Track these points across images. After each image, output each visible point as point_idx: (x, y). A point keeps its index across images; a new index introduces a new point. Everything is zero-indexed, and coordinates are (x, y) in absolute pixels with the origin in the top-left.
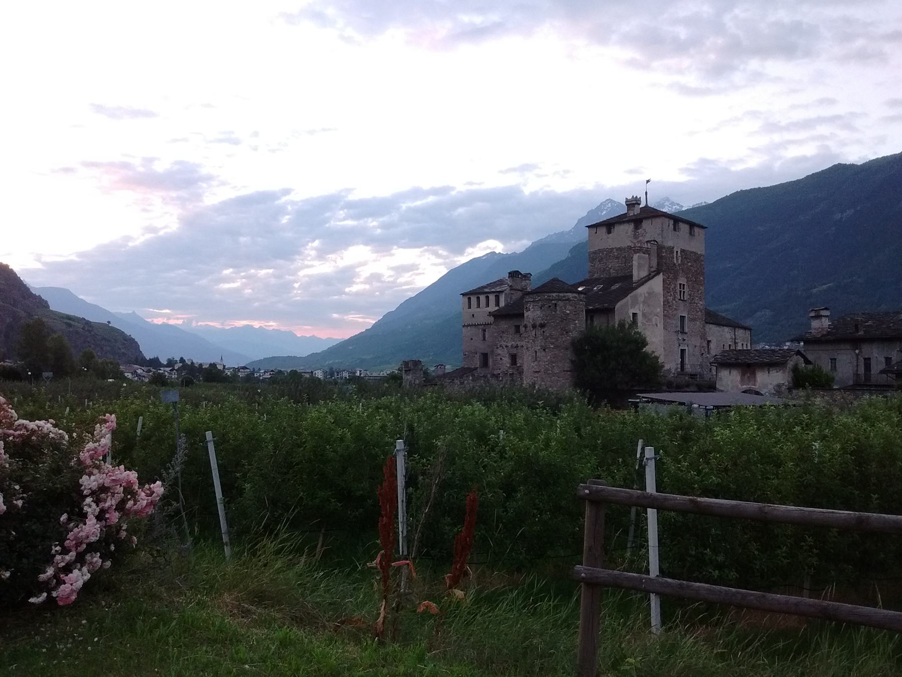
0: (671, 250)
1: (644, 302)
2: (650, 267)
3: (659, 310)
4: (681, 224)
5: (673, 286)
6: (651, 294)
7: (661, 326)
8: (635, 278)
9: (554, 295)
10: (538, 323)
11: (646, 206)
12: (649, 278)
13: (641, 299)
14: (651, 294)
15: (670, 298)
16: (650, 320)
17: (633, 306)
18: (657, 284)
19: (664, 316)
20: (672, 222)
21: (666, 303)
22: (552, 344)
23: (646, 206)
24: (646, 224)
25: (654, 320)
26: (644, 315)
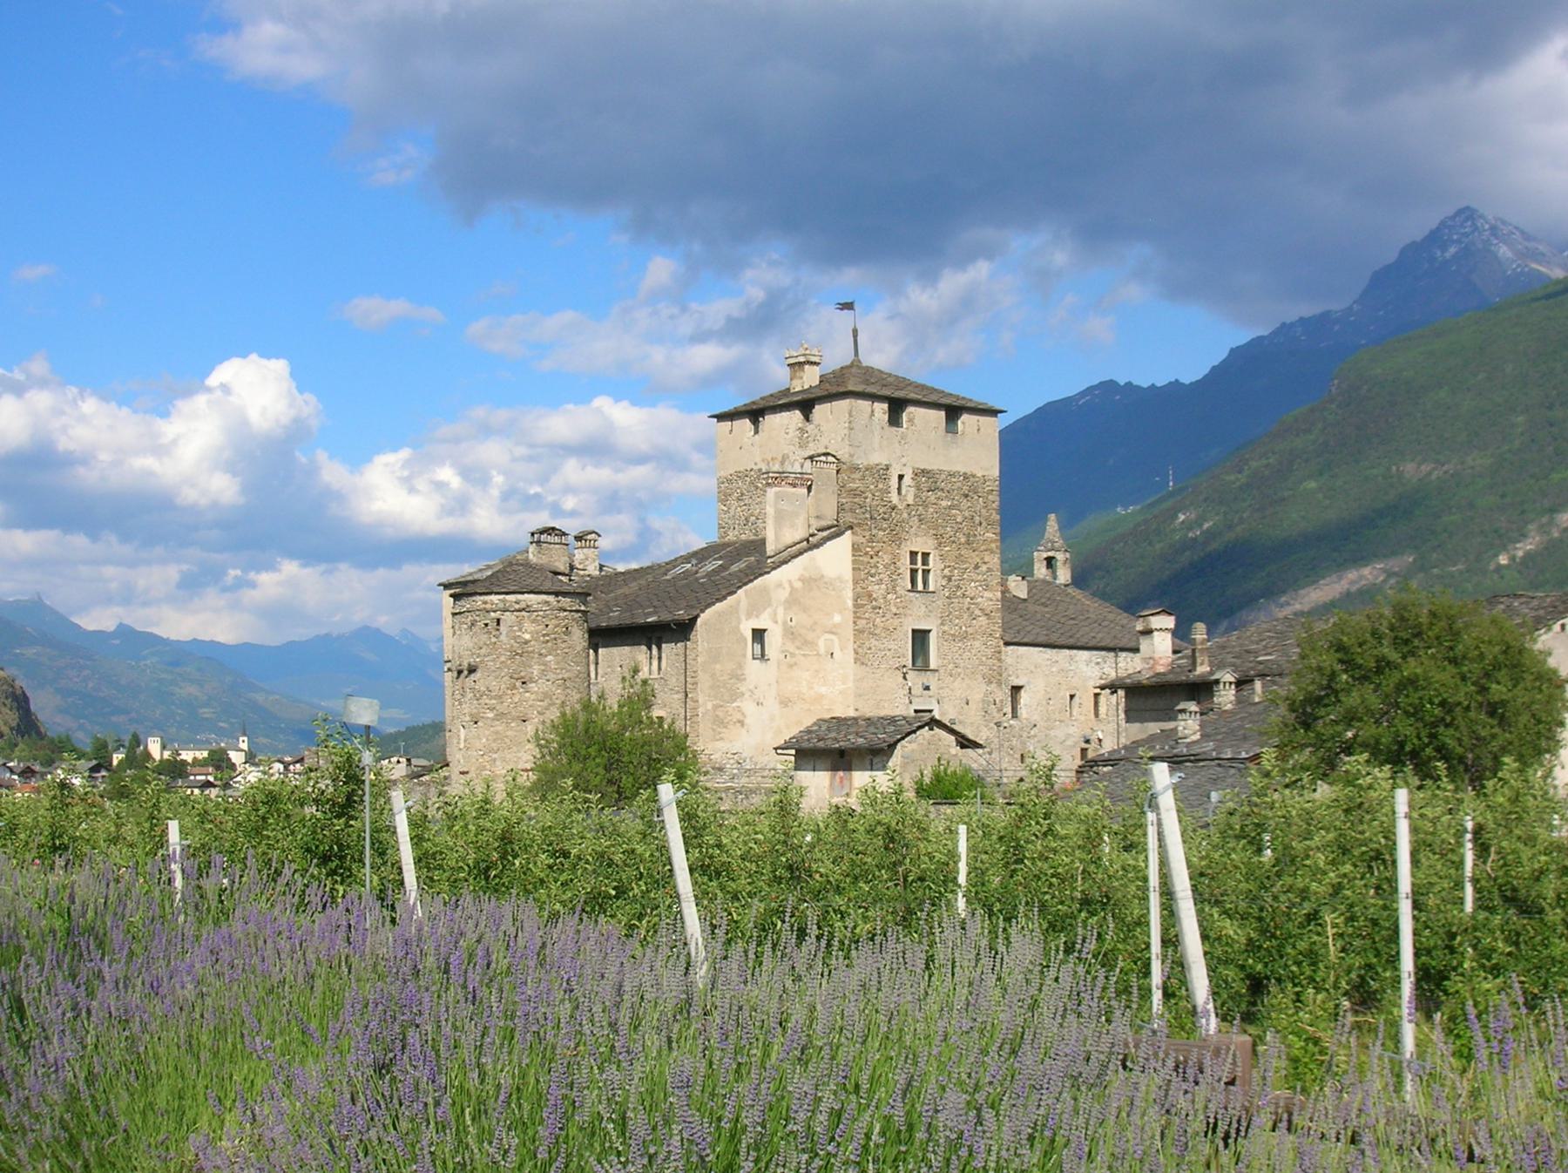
1: (792, 601)
3: (842, 617)
4: (911, 409)
5: (887, 559)
6: (812, 581)
7: (845, 656)
8: (770, 548)
9: (494, 598)
10: (465, 664)
11: (856, 364)
13: (784, 594)
14: (812, 581)
15: (878, 591)
17: (754, 611)
18: (836, 557)
20: (881, 408)
22: (492, 709)
23: (856, 364)
24: (819, 411)
25: (821, 643)
26: (790, 633)
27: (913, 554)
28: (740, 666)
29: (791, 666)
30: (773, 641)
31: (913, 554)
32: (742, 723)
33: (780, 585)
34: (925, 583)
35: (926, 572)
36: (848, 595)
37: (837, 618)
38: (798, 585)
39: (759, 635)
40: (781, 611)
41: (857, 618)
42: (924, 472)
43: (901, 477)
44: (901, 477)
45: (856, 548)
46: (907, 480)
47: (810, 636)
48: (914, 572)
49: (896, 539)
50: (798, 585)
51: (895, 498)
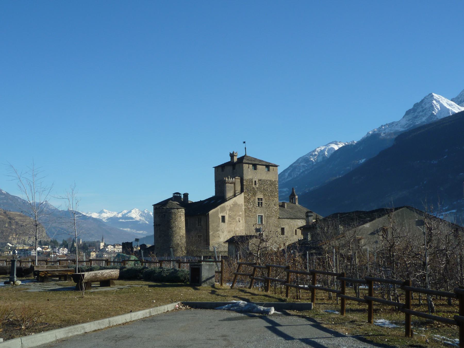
0: (251, 180)
1: (230, 210)
2: (235, 191)
6: (235, 205)
7: (242, 221)
12: (235, 196)
14: (235, 205)
16: (234, 219)
18: (240, 199)
19: (246, 216)
20: (251, 166)
21: (247, 210)
25: (237, 219)
26: (230, 216)
27: (259, 199)
28: (219, 224)
29: (230, 224)
30: (227, 218)
31: (259, 199)
32: (219, 237)
33: (227, 206)
34: (262, 206)
35: (262, 203)
36: (243, 207)
37: (241, 213)
38: (232, 206)
39: (223, 218)
40: (228, 212)
41: (245, 212)
42: (260, 180)
43: (255, 181)
44: (255, 181)
45: (245, 197)
46: (257, 182)
47: (235, 217)
48: (259, 203)
49: (254, 194)
50: (232, 206)
51: (254, 186)
